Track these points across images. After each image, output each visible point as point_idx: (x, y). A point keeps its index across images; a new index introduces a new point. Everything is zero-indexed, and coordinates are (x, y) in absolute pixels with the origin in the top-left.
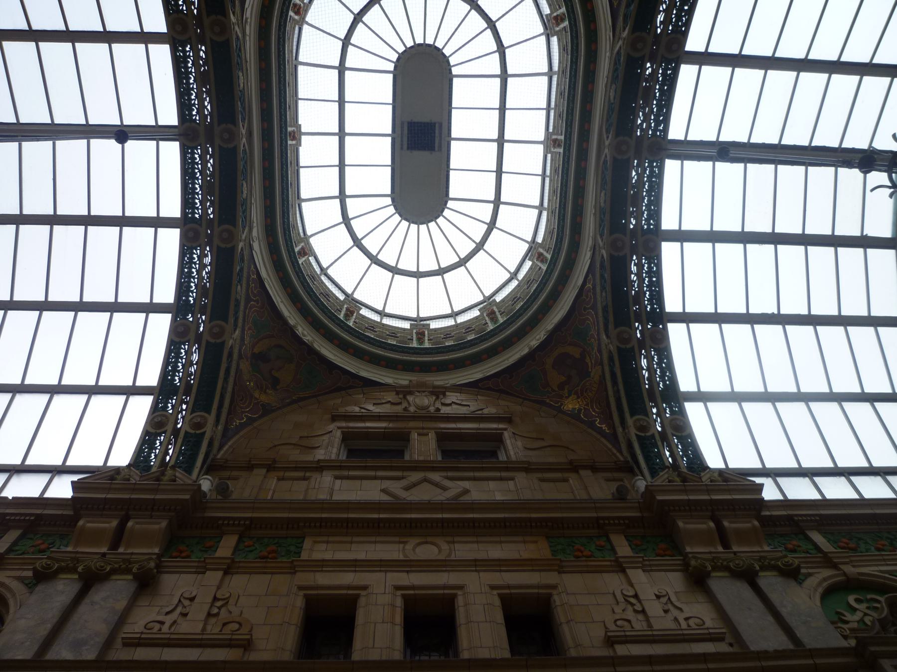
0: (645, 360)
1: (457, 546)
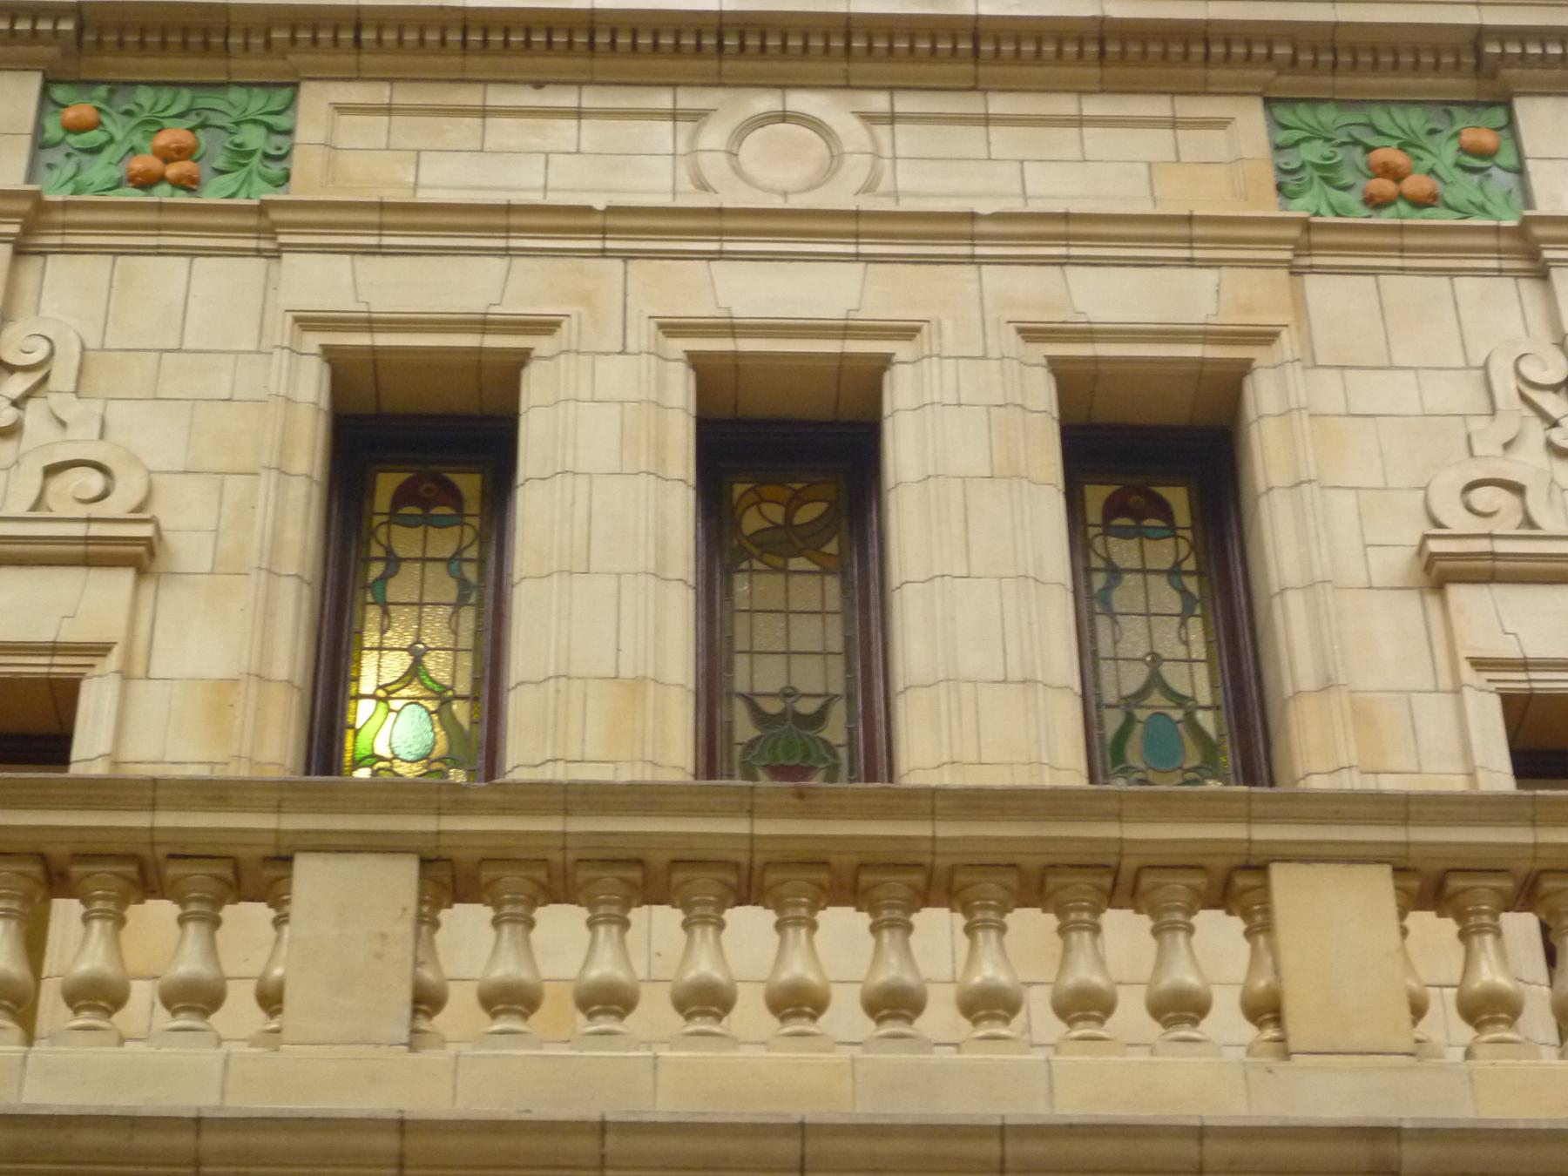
1: (908, 137)
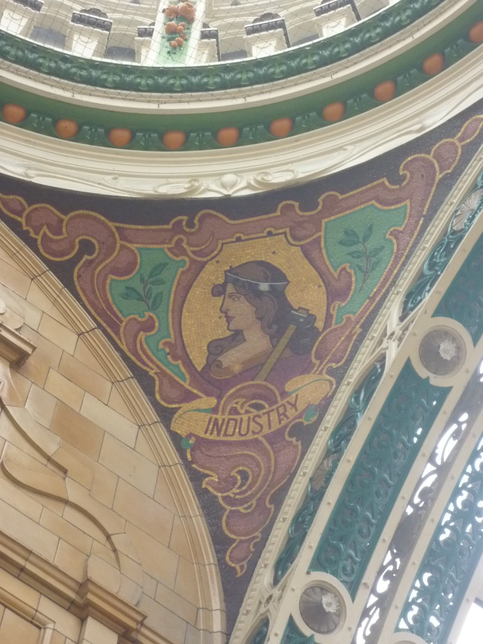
0: (453, 443)
